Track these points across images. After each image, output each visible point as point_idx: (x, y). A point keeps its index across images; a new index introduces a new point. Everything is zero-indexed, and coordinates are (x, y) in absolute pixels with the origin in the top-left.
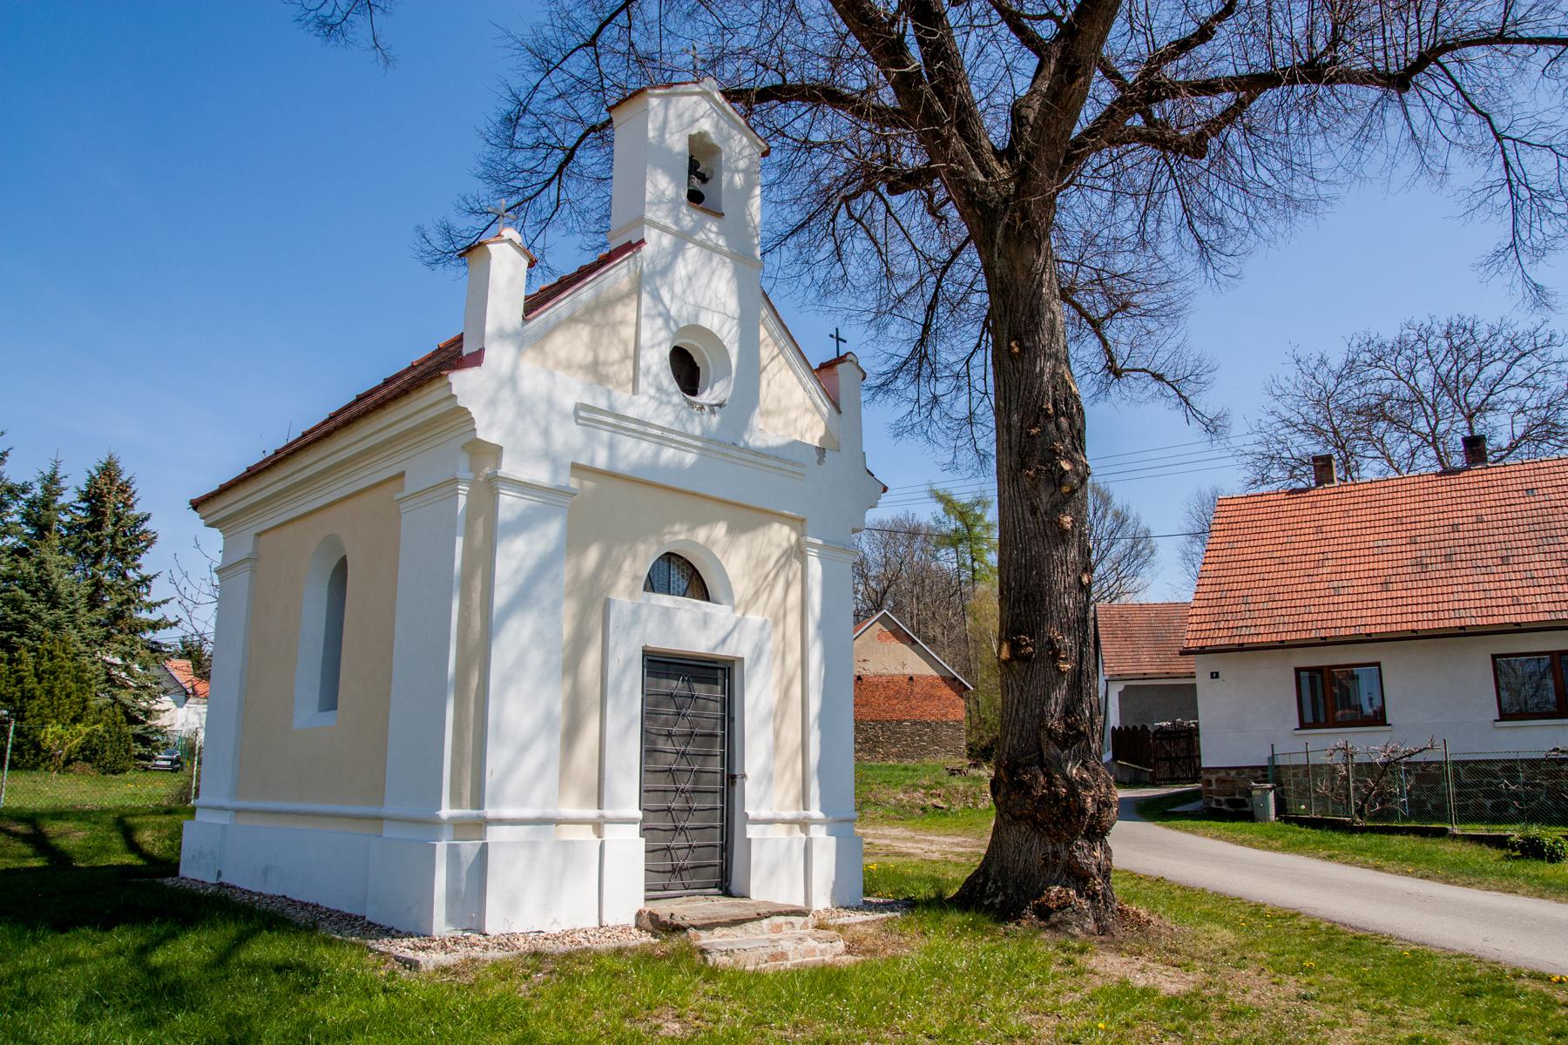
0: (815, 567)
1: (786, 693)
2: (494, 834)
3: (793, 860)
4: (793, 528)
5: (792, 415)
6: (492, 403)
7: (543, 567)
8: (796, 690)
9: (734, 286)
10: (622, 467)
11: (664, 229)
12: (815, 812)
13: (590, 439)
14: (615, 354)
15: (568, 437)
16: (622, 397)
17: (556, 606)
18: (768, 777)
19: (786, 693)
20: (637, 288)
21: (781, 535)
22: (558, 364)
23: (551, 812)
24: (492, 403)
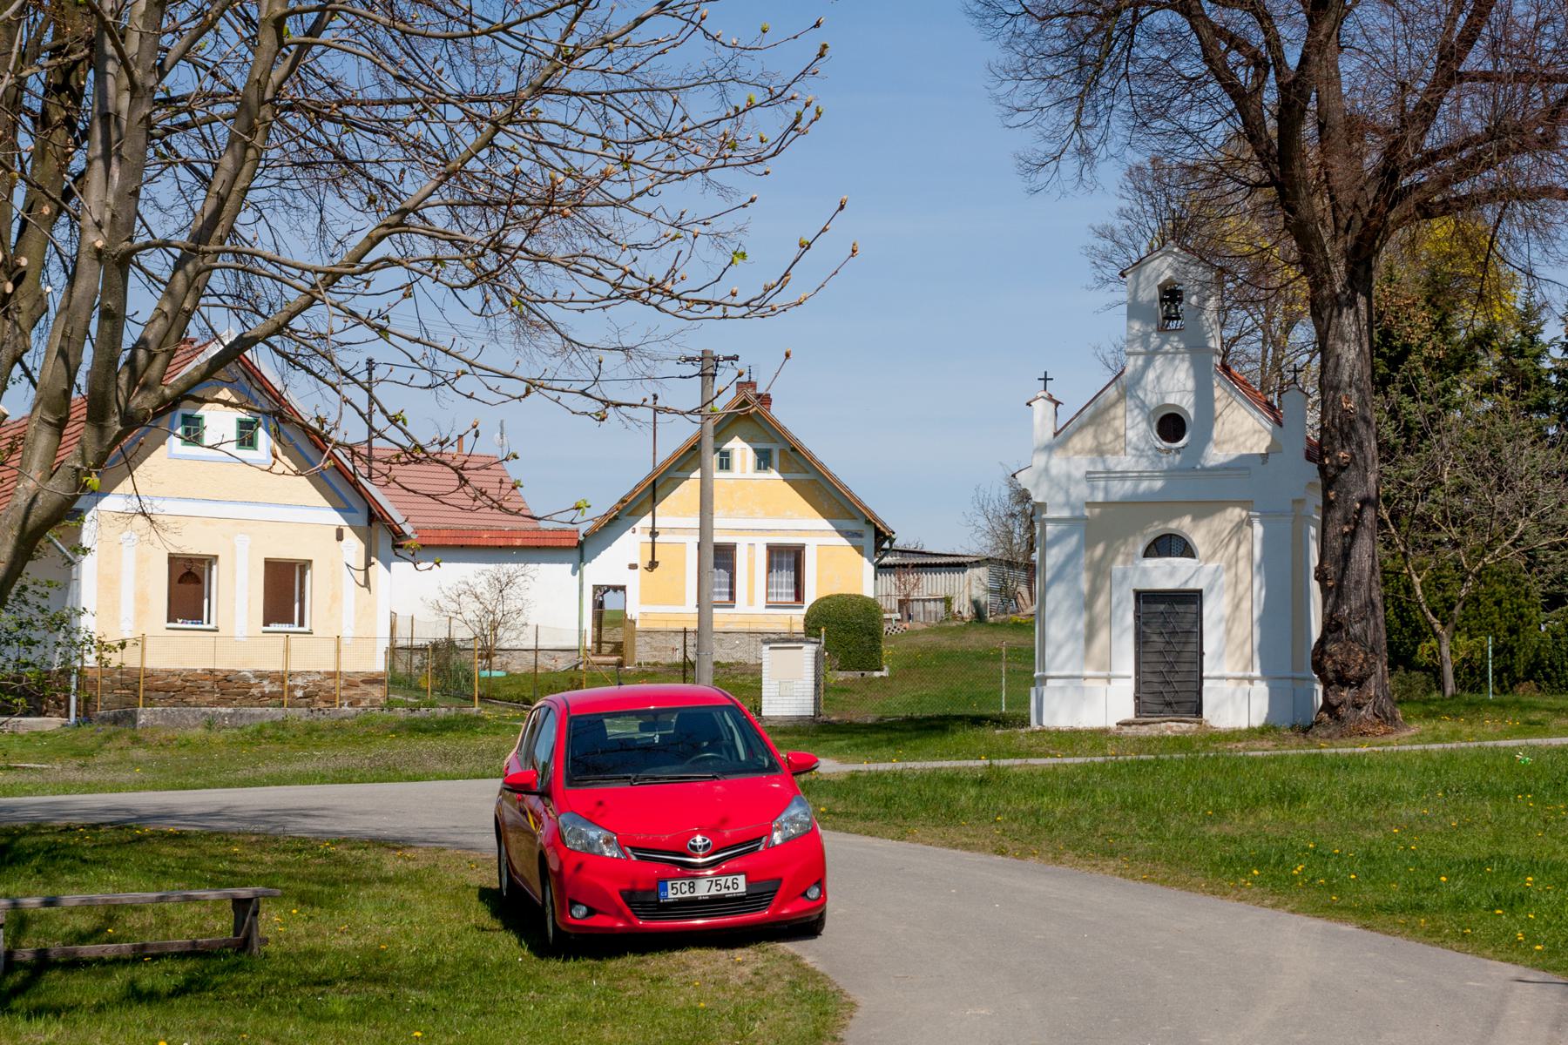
0: (1258, 529)
1: (1237, 607)
2: (1050, 683)
3: (1236, 698)
4: (1243, 508)
5: (1242, 439)
6: (1036, 485)
7: (1071, 558)
8: (1246, 605)
9: (1191, 372)
10: (1115, 497)
11: (1139, 354)
12: (1257, 673)
13: (1093, 488)
14: (1110, 437)
15: (1081, 492)
16: (1113, 462)
17: (1076, 578)
18: (1219, 656)
19: (1237, 607)
20: (1121, 397)
21: (1236, 513)
22: (1076, 453)
23: (1076, 673)
24: (1036, 485)
